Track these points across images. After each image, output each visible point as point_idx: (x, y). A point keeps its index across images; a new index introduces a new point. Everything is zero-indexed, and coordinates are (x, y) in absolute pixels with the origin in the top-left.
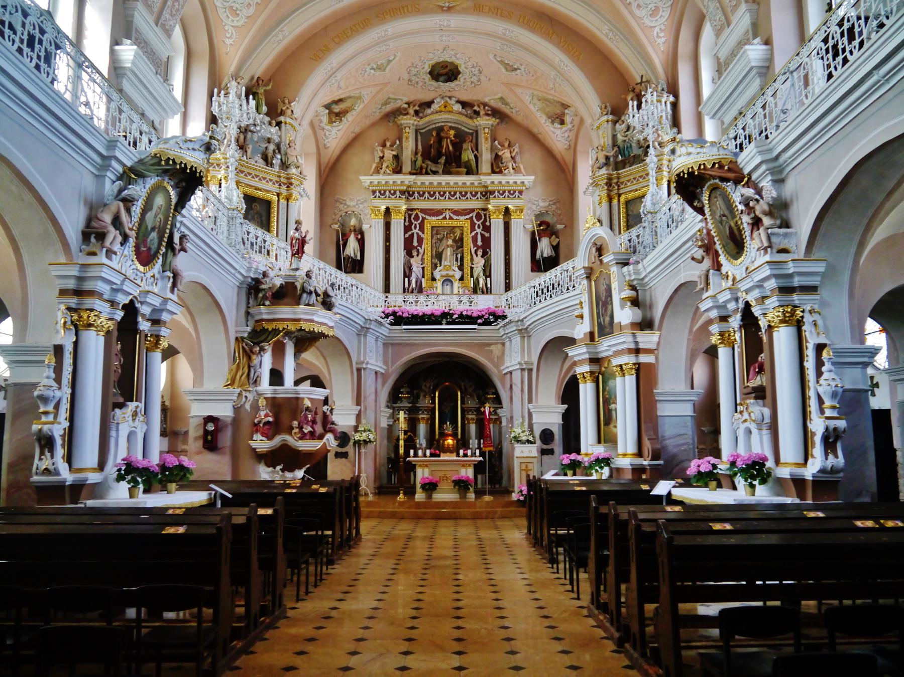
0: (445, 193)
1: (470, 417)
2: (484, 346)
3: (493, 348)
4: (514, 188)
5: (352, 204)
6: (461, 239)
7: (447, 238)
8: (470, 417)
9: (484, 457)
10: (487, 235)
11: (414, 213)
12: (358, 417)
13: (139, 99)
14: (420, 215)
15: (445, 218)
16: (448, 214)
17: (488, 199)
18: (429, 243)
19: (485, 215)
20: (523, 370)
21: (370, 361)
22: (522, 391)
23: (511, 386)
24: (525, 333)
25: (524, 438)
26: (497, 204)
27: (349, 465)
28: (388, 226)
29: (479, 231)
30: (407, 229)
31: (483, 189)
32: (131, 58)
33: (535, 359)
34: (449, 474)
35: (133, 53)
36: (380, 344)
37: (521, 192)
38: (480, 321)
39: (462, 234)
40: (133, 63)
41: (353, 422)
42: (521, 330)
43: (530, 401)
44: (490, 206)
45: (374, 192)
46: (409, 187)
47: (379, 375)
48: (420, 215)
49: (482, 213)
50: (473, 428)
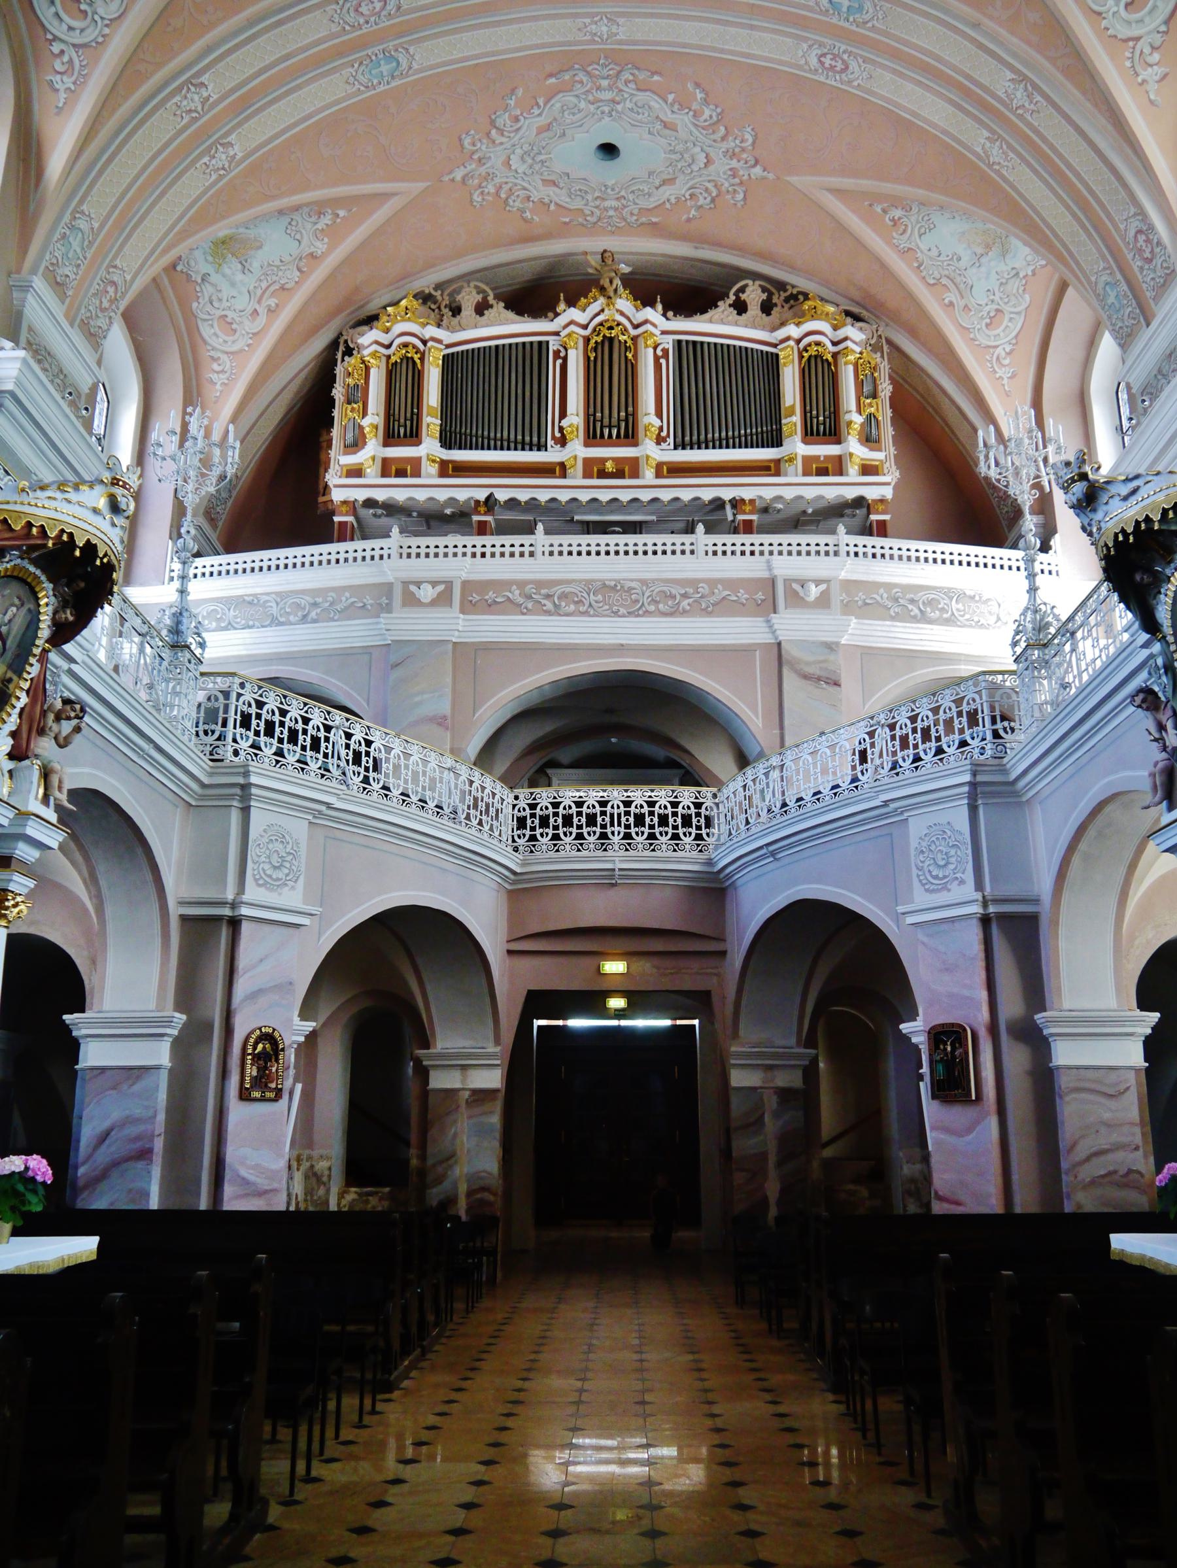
13: (29, 452)
32: (15, 373)
35: (18, 365)
40: (18, 383)
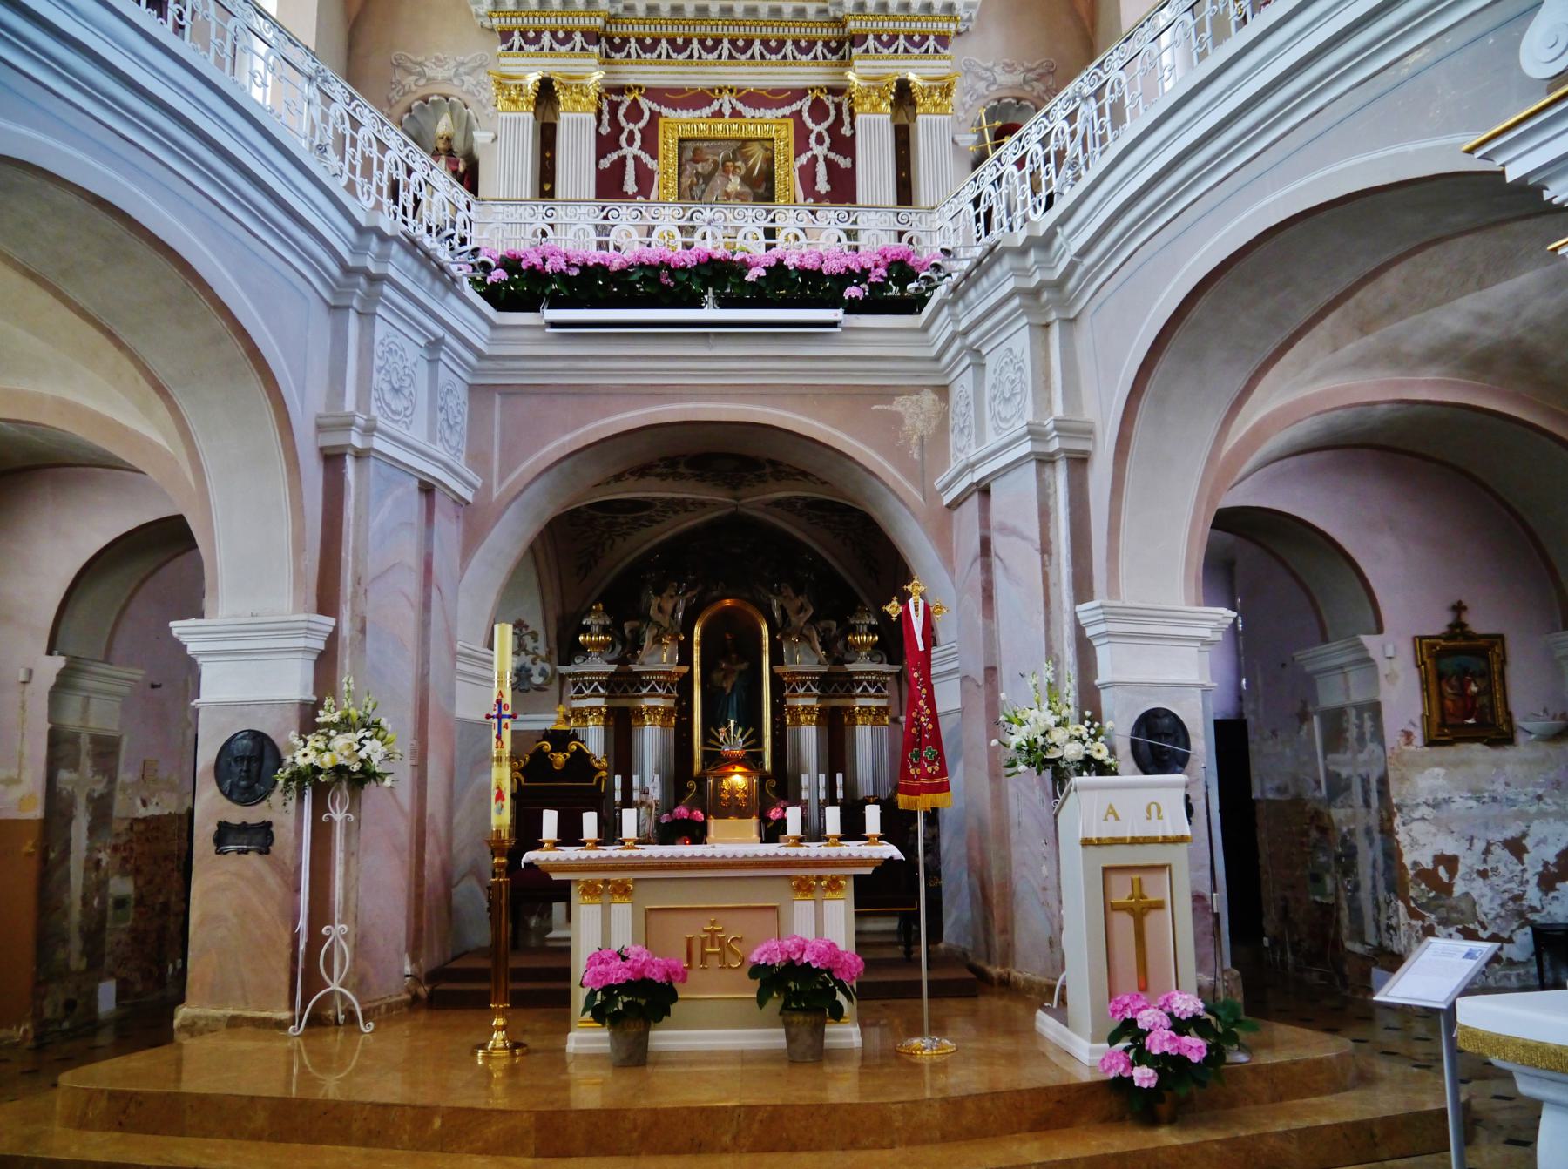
0: (718, 41)
1: (800, 702)
2: (865, 399)
3: (900, 405)
4: (924, 26)
5: (439, 73)
6: (768, 176)
7: (725, 171)
8: (800, 702)
9: (908, 847)
10: (844, 163)
11: (627, 100)
12: (326, 663)
14: (645, 104)
15: (719, 114)
16: (726, 103)
17: (846, 62)
18: (673, 185)
19: (838, 107)
20: (1044, 461)
21: (382, 423)
22: (1046, 549)
23: (986, 544)
24: (1050, 305)
25: (1073, 751)
26: (873, 72)
27: (273, 882)
28: (547, 137)
29: (820, 151)
30: (605, 144)
31: (832, 32)
33: (1103, 410)
34: (733, 928)
36: (453, 380)
37: (943, 40)
38: (852, 292)
39: (770, 161)
41: (292, 682)
42: (1035, 293)
43: (1082, 589)
44: (851, 76)
45: (506, 35)
46: (611, 19)
47: (438, 496)
48: (645, 104)
49: (829, 101)
50: (809, 738)
